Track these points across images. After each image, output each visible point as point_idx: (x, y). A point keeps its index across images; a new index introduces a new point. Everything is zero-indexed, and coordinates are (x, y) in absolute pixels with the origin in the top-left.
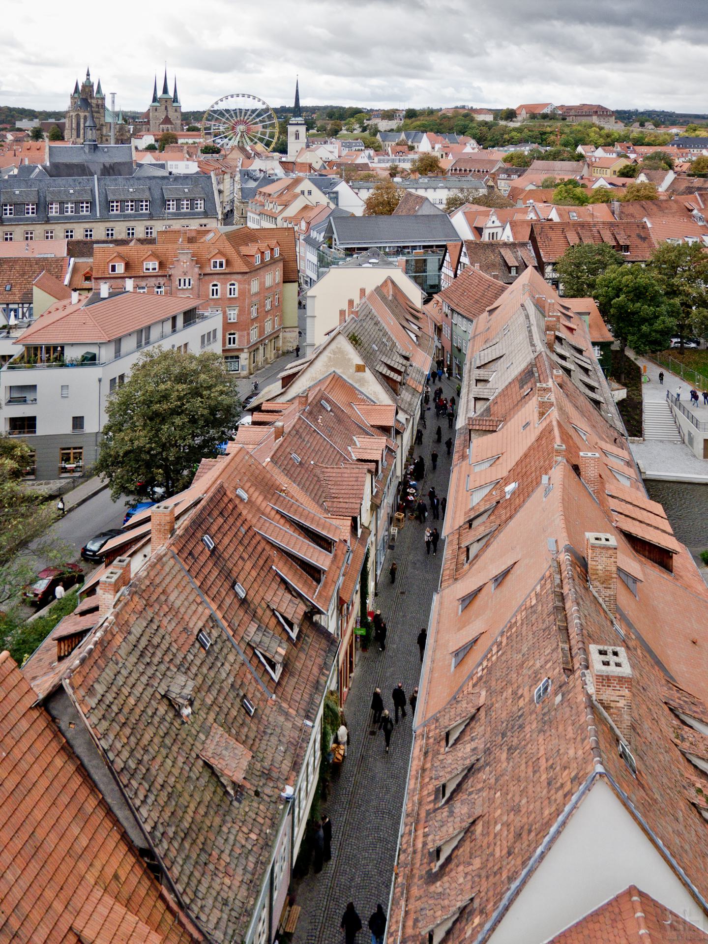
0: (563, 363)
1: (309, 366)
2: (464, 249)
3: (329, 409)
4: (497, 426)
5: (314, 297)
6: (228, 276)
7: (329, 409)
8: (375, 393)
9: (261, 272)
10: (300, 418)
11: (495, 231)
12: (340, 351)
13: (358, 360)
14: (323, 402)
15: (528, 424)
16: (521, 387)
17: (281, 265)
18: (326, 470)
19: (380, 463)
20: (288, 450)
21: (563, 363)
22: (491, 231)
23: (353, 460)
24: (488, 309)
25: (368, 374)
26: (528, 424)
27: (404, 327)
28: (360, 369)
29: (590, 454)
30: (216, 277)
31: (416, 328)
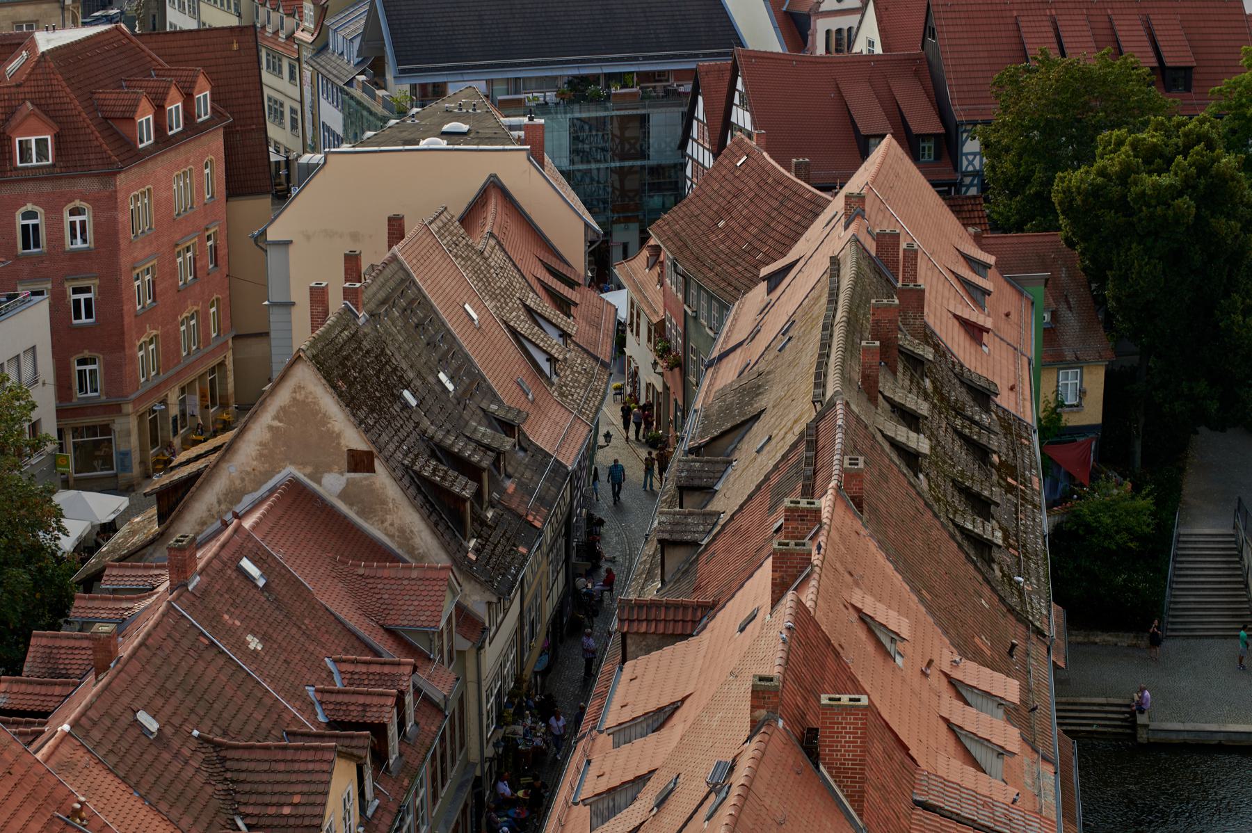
0: (903, 434)
1: (221, 459)
2: (739, 86)
3: (261, 583)
4: (695, 623)
5: (287, 243)
6: (65, 186)
7: (261, 583)
8: (402, 530)
9: (159, 167)
10: (170, 607)
11: (844, 22)
12: (303, 410)
13: (354, 439)
14: (246, 564)
15: (752, 617)
16: (772, 508)
17: (215, 143)
18: (230, 754)
19: (393, 730)
20: (126, 700)
21: (903, 434)
22: (834, 23)
23: (318, 724)
24: (765, 271)
25: (382, 479)
26: (752, 617)
27: (514, 332)
28: (360, 462)
29: (845, 699)
30: (31, 188)
31: (553, 334)
